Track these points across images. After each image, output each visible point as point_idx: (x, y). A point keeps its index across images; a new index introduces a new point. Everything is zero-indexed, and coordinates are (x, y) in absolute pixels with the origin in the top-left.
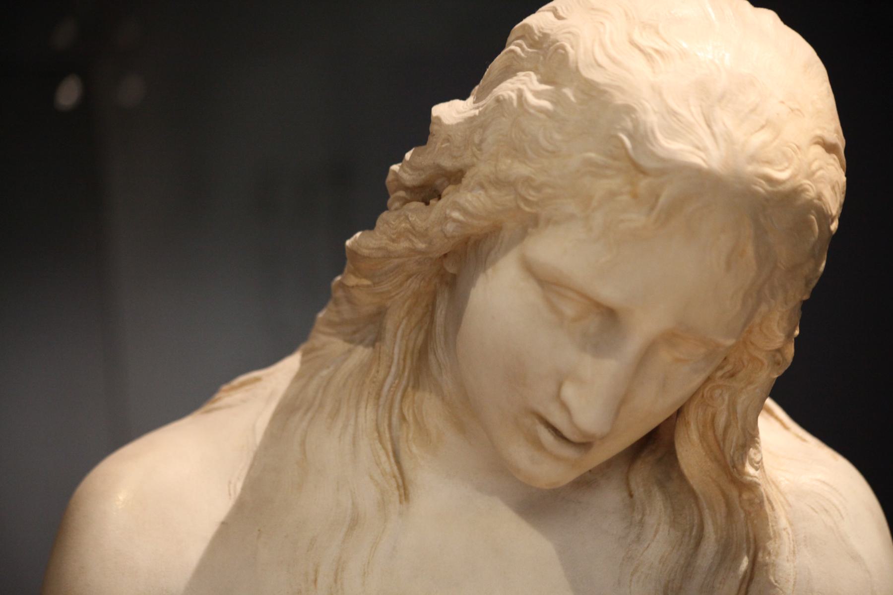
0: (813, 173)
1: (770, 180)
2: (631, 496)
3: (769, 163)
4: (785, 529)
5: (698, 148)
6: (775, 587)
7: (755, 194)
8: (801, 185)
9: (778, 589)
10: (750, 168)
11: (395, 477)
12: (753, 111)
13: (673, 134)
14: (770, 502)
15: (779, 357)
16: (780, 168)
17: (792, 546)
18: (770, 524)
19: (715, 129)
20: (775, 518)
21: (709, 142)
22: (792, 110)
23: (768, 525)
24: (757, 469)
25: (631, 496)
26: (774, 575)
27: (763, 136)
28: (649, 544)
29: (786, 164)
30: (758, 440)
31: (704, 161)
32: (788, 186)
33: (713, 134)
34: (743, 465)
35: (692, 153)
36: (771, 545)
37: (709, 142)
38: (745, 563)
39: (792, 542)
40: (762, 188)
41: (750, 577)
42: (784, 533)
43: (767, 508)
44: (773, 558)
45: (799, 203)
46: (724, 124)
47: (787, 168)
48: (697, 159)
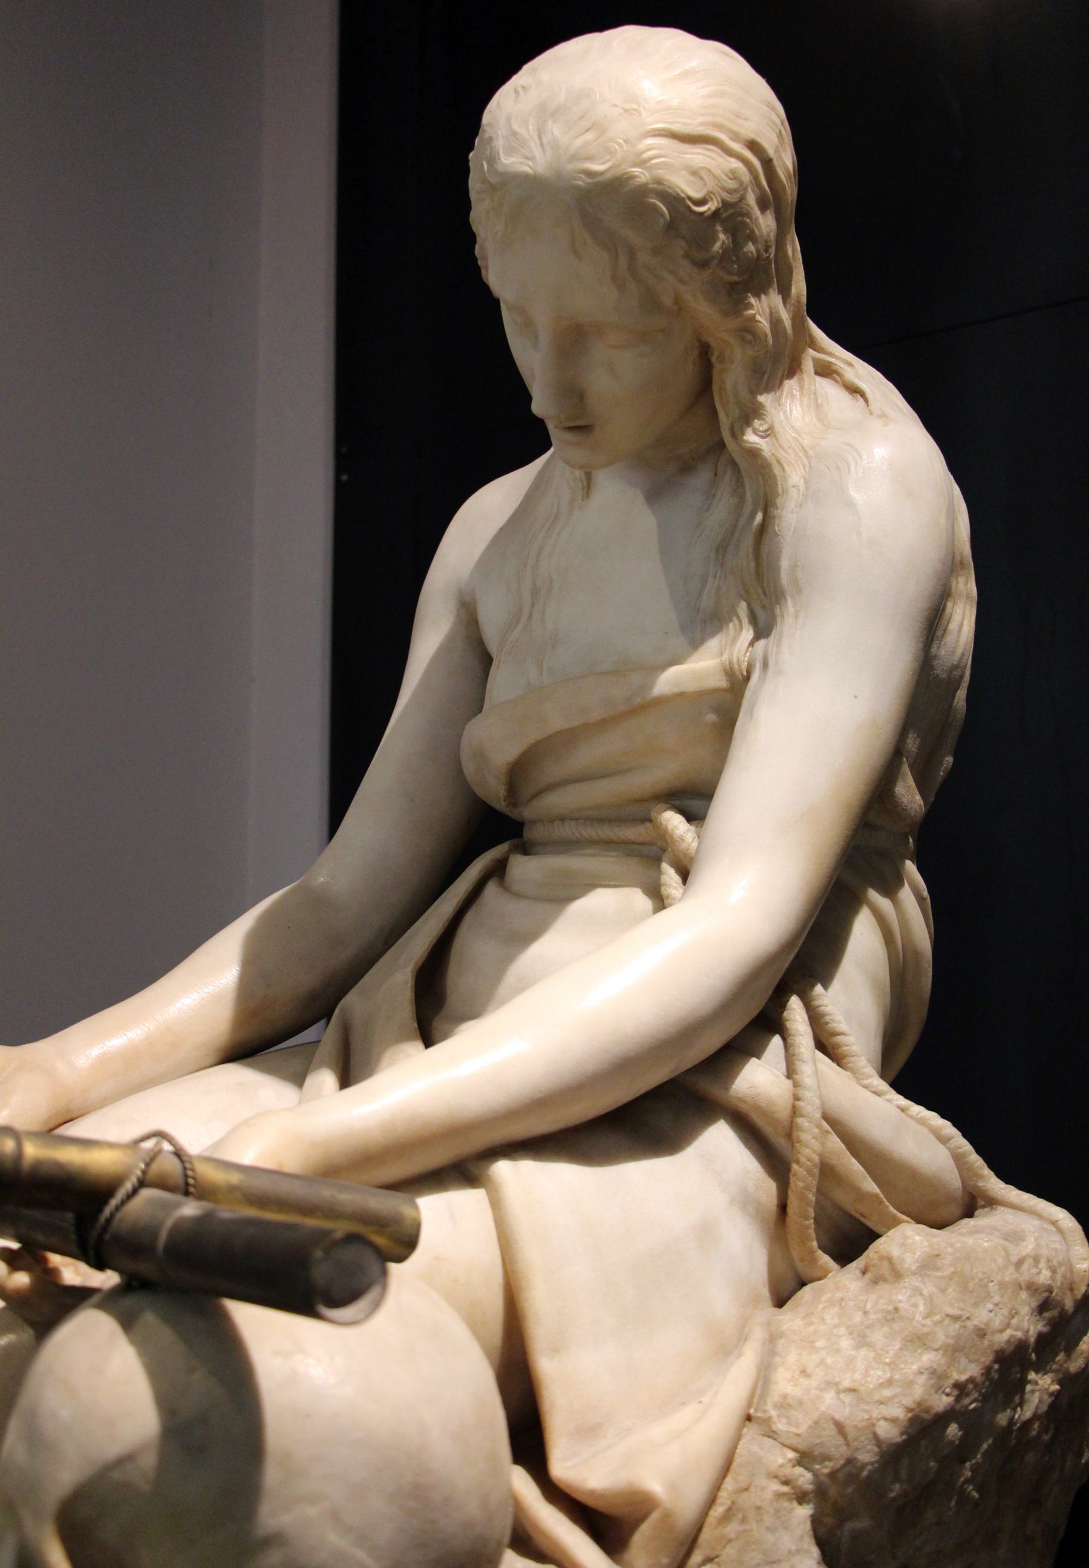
0: (645, 161)
1: (590, 174)
2: (716, 475)
3: (590, 158)
4: (793, 487)
5: (527, 158)
6: (778, 535)
7: (577, 188)
8: (626, 173)
9: (780, 537)
10: (570, 167)
11: (582, 482)
12: (581, 118)
13: (511, 151)
14: (781, 465)
15: (749, 337)
16: (604, 160)
17: (800, 499)
18: (779, 483)
19: (544, 140)
20: (785, 477)
21: (537, 152)
22: (626, 111)
23: (777, 484)
24: (762, 437)
25: (716, 475)
26: (778, 525)
27: (589, 136)
28: (713, 511)
29: (608, 157)
30: (765, 413)
31: (530, 167)
32: (608, 176)
33: (542, 145)
34: (743, 434)
35: (521, 163)
36: (779, 501)
37: (537, 152)
38: (759, 517)
39: (801, 497)
40: (582, 182)
41: (763, 528)
42: (793, 492)
43: (777, 471)
44: (779, 511)
45: (627, 189)
46: (553, 134)
47: (608, 161)
48: (526, 168)
